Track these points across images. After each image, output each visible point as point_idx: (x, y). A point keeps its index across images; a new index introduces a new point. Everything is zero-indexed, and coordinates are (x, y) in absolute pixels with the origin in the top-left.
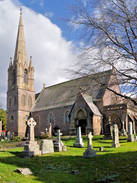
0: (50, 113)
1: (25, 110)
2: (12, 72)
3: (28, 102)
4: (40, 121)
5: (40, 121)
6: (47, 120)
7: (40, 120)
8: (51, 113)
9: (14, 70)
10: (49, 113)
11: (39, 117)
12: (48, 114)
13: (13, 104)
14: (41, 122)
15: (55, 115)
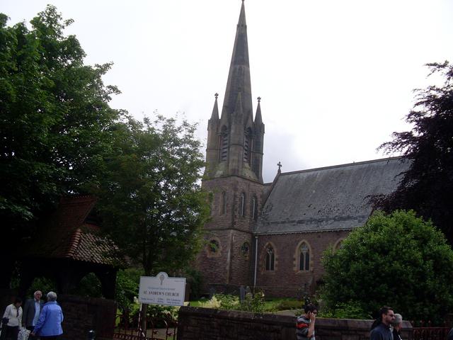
0: (300, 243)
1: (245, 230)
2: (220, 131)
3: (251, 210)
4: (277, 260)
5: (277, 260)
6: (295, 259)
7: (276, 256)
8: (304, 243)
9: (225, 126)
10: (299, 241)
11: (275, 250)
12: (297, 244)
13: (220, 211)
14: (279, 263)
15: (313, 249)
